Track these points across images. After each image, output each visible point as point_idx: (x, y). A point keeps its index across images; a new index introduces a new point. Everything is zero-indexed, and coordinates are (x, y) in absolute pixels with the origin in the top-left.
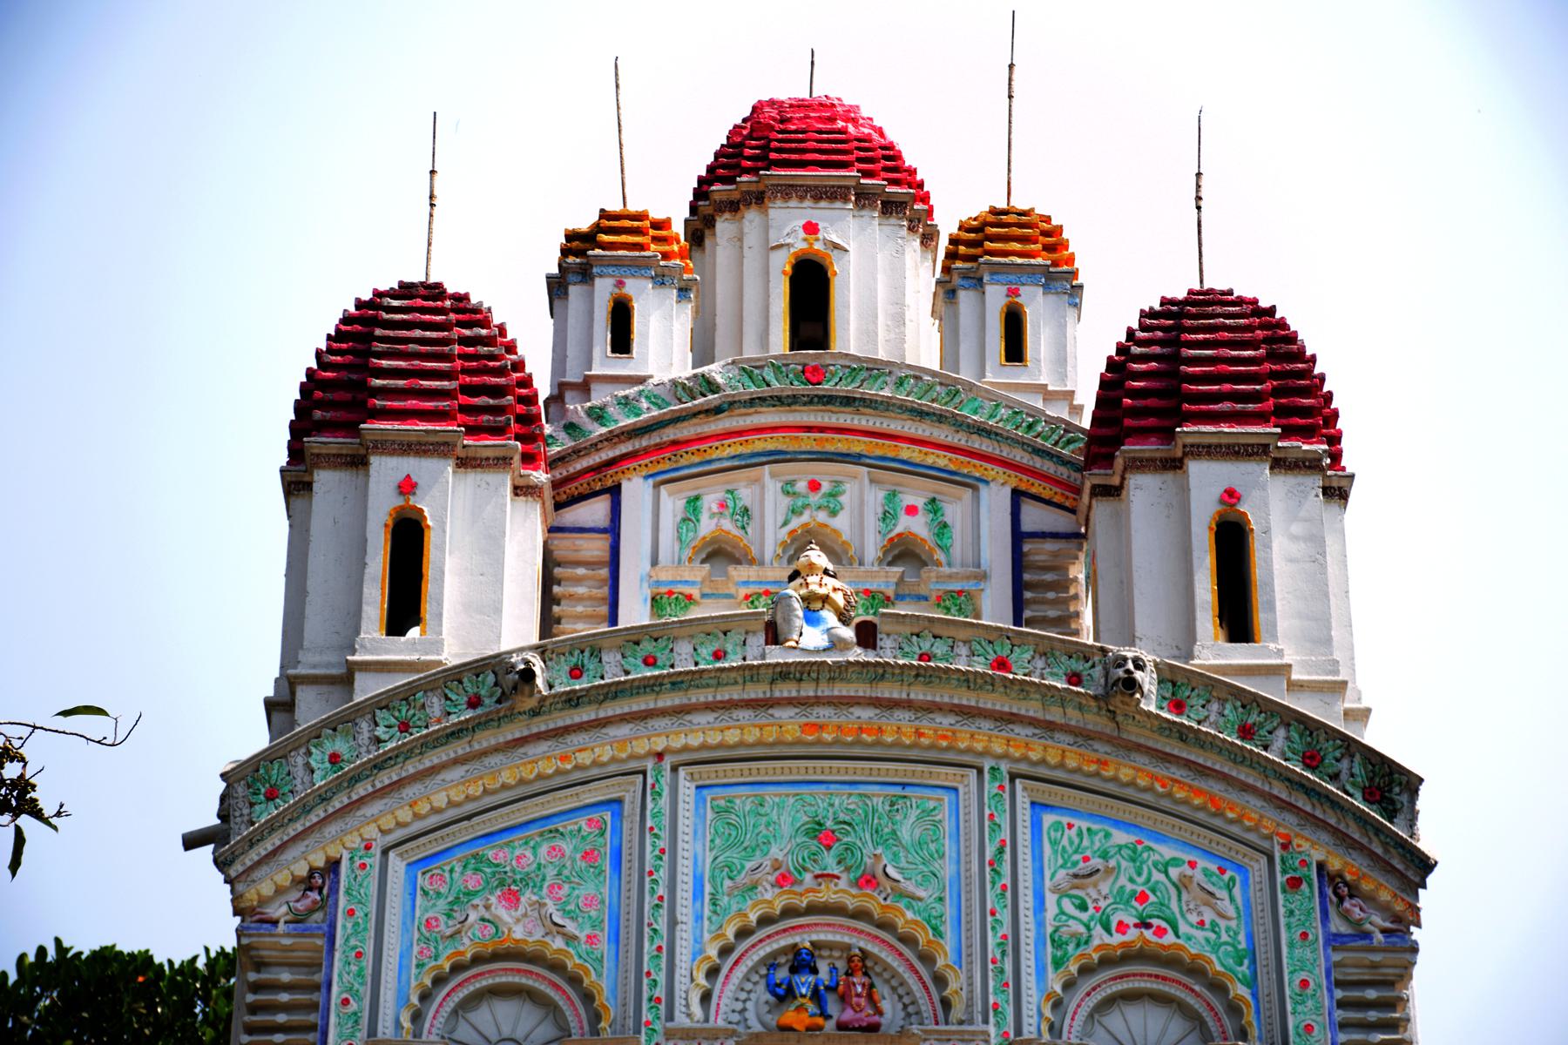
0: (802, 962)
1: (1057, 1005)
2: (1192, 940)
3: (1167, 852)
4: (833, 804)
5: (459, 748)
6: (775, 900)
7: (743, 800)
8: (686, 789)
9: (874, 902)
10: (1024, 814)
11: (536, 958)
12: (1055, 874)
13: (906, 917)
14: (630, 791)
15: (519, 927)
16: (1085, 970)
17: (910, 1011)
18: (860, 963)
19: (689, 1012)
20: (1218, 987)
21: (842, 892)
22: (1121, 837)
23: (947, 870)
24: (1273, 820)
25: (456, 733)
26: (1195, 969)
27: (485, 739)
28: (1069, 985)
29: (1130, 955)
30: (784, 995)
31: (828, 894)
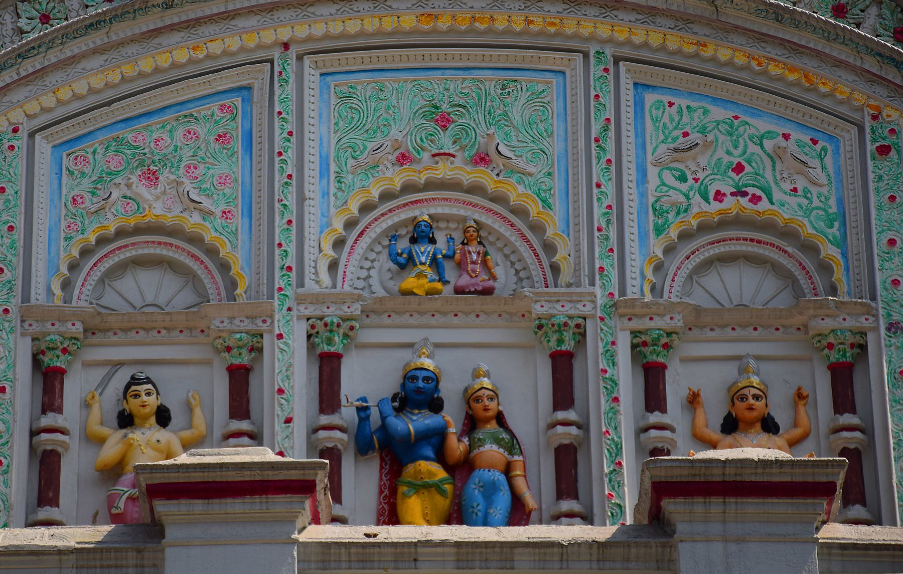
0: (421, 234)
1: (659, 268)
2: (784, 207)
3: (762, 125)
4: (446, 89)
5: (97, 38)
6: (397, 178)
7: (364, 85)
8: (311, 76)
9: (485, 177)
10: (628, 94)
11: (174, 232)
12: (657, 148)
13: (516, 192)
14: (258, 77)
15: (158, 206)
16: (685, 236)
17: (522, 276)
18: (474, 234)
19: (319, 279)
20: (810, 248)
21: (458, 170)
22: (719, 113)
23: (557, 147)
24: (862, 95)
25: (94, 25)
26: (789, 234)
27: (122, 30)
28: (669, 250)
29: (726, 222)
30: (406, 263)
31: (443, 171)
